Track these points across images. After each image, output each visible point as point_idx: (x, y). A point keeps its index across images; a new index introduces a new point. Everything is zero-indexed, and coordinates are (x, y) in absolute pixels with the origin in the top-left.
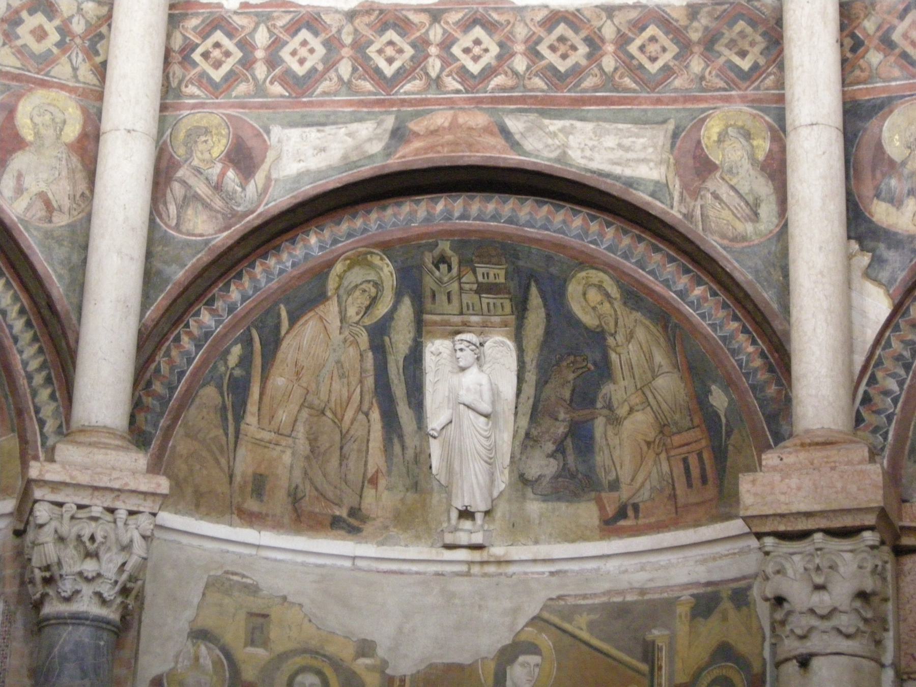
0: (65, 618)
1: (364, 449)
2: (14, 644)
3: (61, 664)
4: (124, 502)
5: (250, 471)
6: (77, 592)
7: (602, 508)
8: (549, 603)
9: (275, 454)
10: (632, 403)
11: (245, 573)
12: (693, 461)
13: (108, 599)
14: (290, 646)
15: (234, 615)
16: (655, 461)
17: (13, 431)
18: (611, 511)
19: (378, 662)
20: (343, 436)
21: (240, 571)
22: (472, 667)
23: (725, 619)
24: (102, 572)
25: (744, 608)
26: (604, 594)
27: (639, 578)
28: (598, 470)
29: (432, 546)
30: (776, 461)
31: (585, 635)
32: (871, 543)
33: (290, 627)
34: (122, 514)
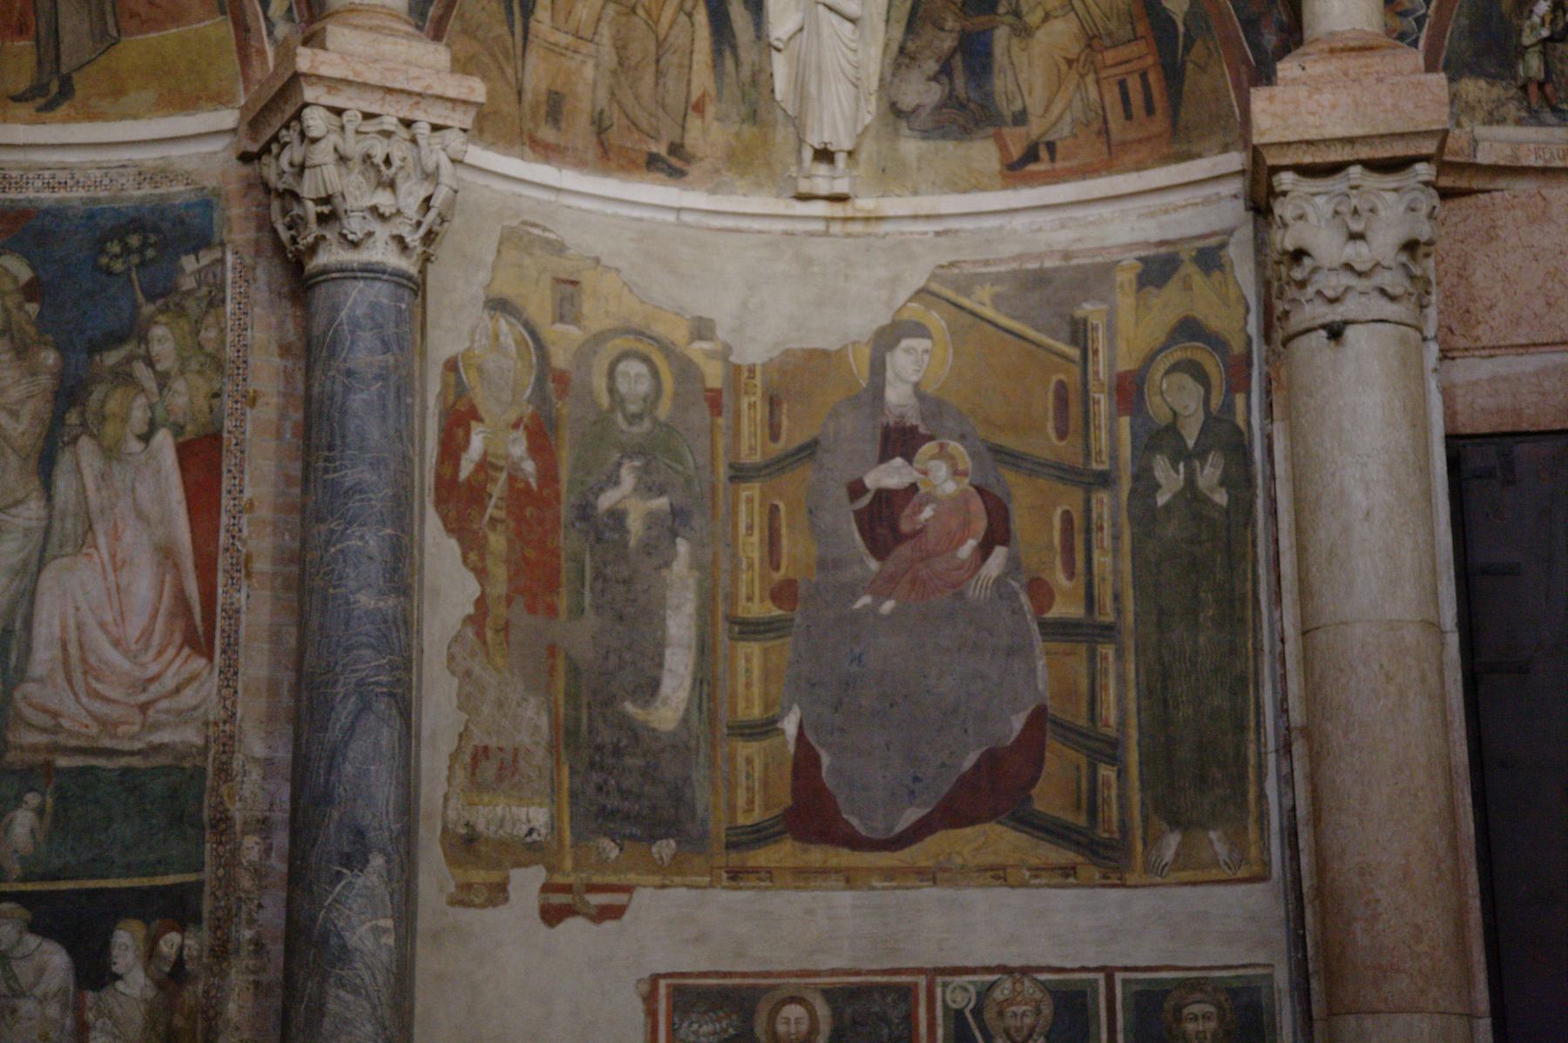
0: (353, 270)
1: (686, 62)
2: (256, 310)
3: (352, 332)
5: (543, 87)
6: (370, 234)
7: (1003, 148)
8: (938, 271)
9: (573, 65)
10: (1049, 6)
12: (1134, 84)
13: (412, 245)
14: (607, 323)
15: (538, 280)
16: (1078, 86)
17: (223, 13)
18: (1016, 152)
20: (659, 45)
21: (539, 221)
22: (840, 354)
23: (1187, 287)
25: (1216, 275)
27: (1062, 238)
29: (778, 196)
30: (1298, 72)
31: (989, 312)
32: (1426, 178)
33: (607, 300)
34: (422, 129)
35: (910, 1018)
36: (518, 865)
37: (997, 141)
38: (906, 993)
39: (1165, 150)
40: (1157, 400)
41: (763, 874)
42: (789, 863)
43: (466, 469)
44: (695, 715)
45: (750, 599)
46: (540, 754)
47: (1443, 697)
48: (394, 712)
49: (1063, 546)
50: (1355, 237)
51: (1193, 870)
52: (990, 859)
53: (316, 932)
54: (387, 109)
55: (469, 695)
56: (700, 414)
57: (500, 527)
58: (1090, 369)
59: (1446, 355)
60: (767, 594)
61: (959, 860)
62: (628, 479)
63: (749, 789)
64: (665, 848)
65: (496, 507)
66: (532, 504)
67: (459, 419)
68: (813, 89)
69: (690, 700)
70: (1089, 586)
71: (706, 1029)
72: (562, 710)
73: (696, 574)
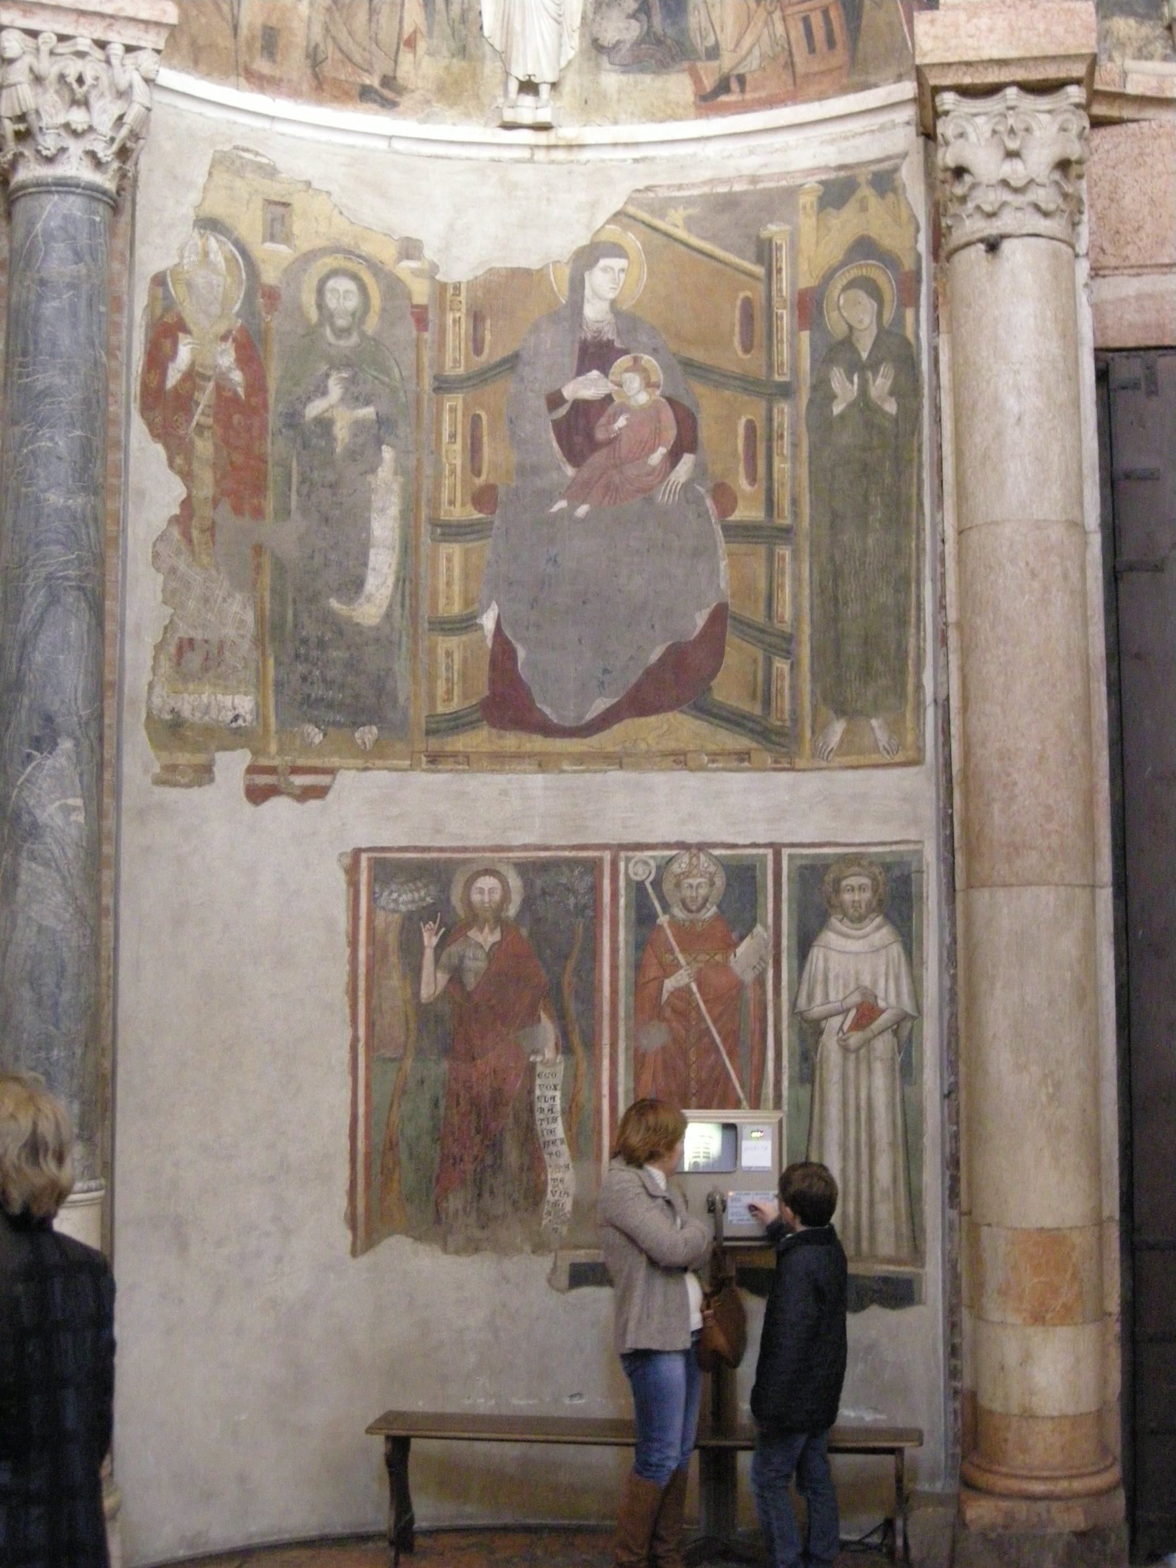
0: (48, 185)
4: (119, 33)
5: (259, 22)
6: (63, 150)
7: (697, 80)
8: (634, 195)
11: (260, 151)
12: (817, 20)
13: (104, 160)
14: (320, 243)
15: (248, 202)
16: (766, 23)
18: (709, 84)
19: (426, 266)
23: (864, 208)
24: (95, 125)
25: (890, 196)
26: (705, 183)
28: (692, 34)
29: (486, 125)
31: (681, 234)
32: (1077, 100)
34: (116, 50)
35: (596, 888)
36: (225, 748)
37: (691, 75)
38: (593, 867)
39: (845, 81)
40: (835, 315)
41: (461, 759)
42: (486, 748)
43: (173, 377)
44: (397, 612)
45: (452, 503)
46: (246, 645)
47: (1084, 594)
48: (83, 604)
49: (746, 453)
50: (1012, 155)
51: (855, 757)
52: (673, 745)
53: (10, 809)
54: (81, 31)
55: (174, 592)
56: (406, 330)
57: (207, 434)
58: (774, 287)
59: (1096, 272)
60: (469, 498)
61: (643, 746)
62: (335, 390)
63: (449, 680)
64: (368, 734)
65: (203, 414)
66: (240, 413)
67: (166, 331)
68: (517, 26)
69: (393, 597)
70: (770, 491)
71: (404, 898)
72: (268, 606)
73: (400, 479)
